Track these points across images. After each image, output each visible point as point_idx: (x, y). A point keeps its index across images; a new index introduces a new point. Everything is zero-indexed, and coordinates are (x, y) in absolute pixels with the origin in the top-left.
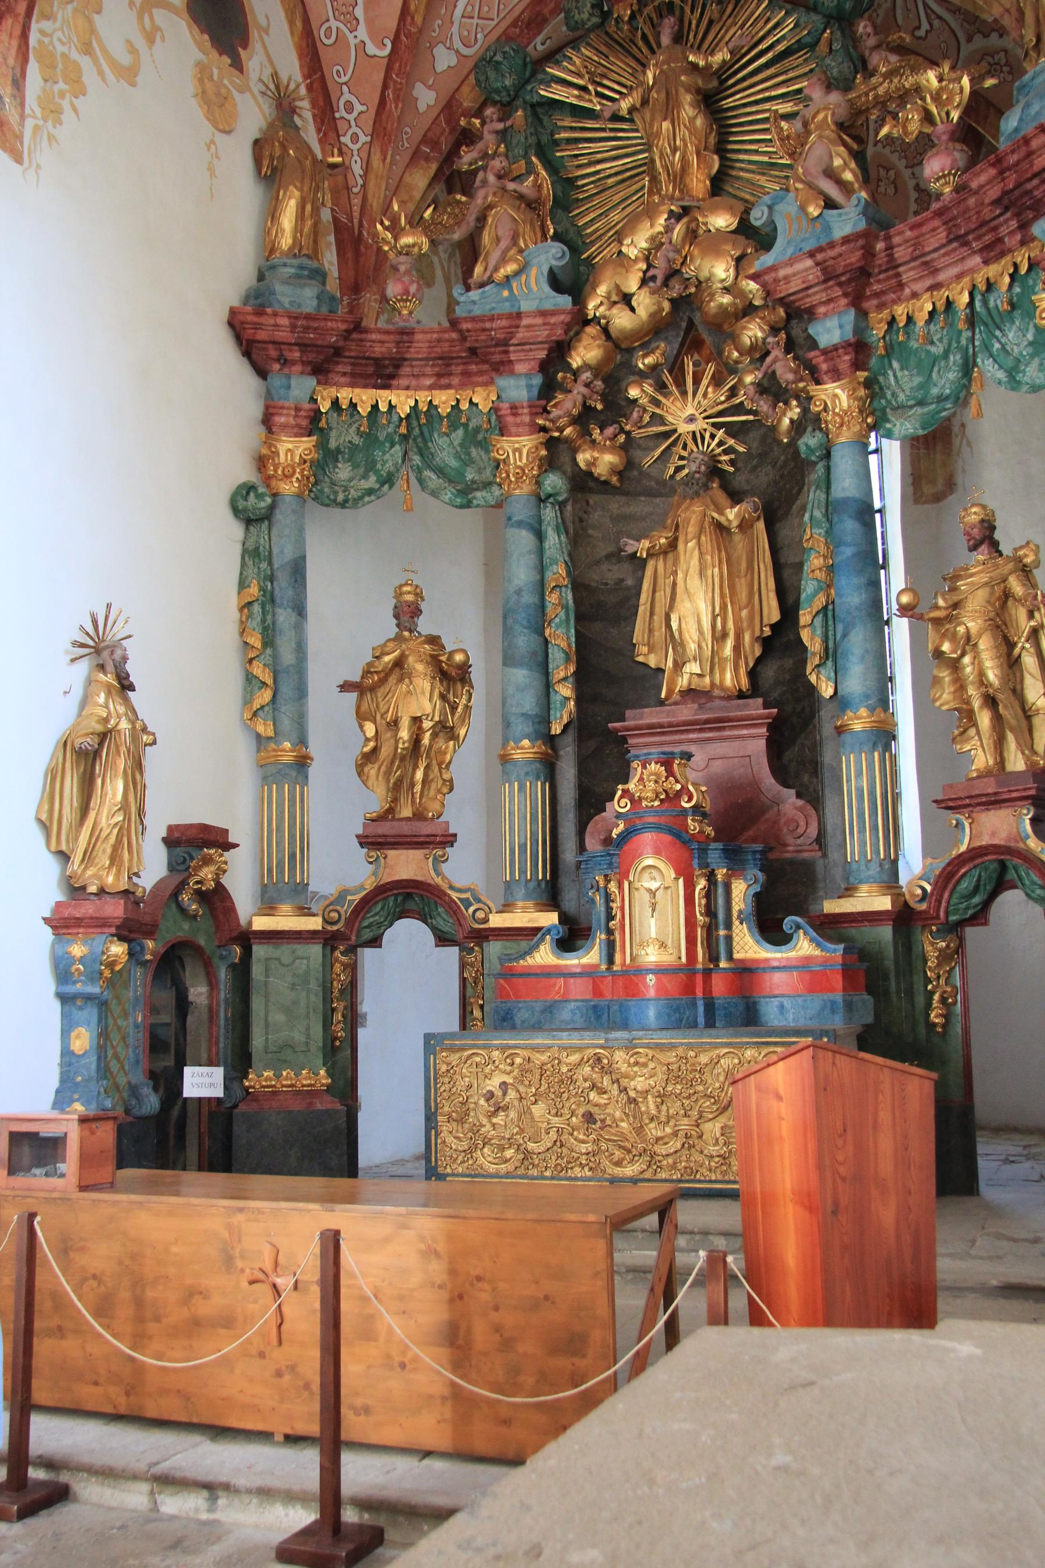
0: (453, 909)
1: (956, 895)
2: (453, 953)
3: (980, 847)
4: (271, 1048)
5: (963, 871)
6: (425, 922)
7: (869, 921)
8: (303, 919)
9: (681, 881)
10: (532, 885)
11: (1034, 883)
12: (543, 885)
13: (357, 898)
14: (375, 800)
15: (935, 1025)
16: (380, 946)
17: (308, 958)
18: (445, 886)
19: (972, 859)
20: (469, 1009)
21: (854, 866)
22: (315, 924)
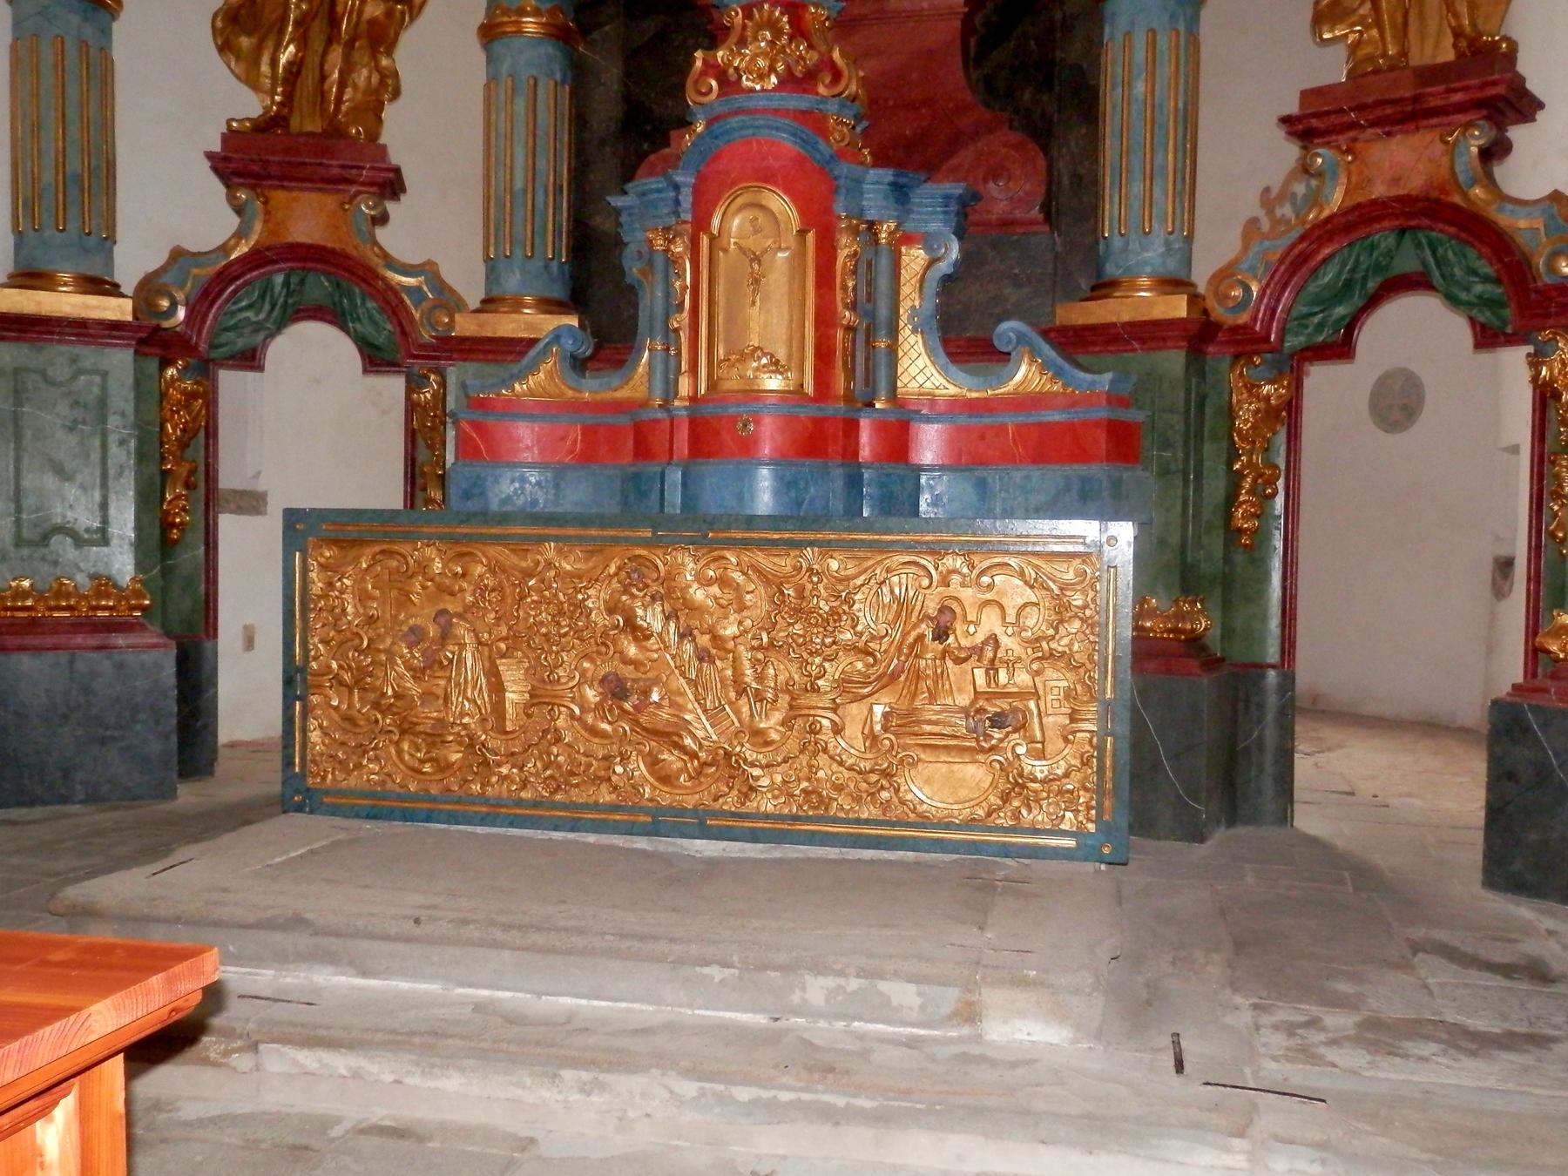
0: (391, 301)
1: (1305, 296)
2: (393, 386)
3: (1374, 203)
4: (26, 533)
5: (1326, 251)
6: (344, 328)
7: (1142, 341)
8: (93, 300)
9: (811, 236)
10: (537, 264)
11: (1474, 272)
12: (554, 266)
13: (211, 270)
14: (250, 105)
15: (1240, 531)
16: (260, 368)
17: (104, 375)
18: (377, 262)
19: (1348, 229)
20: (419, 481)
21: (1117, 243)
22: (118, 309)
